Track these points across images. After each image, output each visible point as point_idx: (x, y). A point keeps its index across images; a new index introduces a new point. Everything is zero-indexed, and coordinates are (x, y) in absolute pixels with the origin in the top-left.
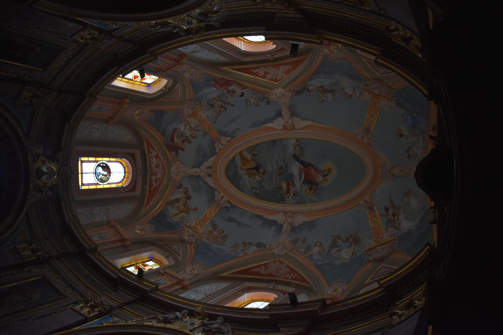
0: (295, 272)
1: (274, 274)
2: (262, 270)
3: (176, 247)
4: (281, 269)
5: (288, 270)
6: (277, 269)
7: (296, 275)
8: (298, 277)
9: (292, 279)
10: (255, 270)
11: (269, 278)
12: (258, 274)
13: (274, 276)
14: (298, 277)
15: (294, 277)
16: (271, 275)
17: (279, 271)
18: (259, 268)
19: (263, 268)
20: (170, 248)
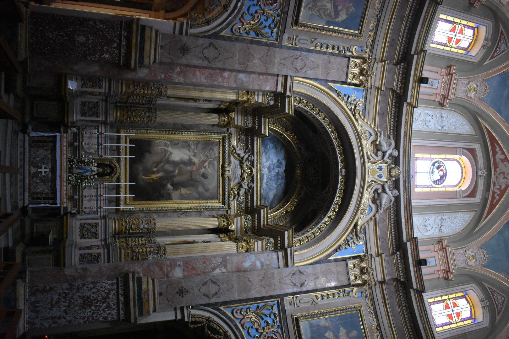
0: (501, 196)
1: (498, 170)
2: (499, 156)
3: (502, 47)
4: (505, 178)
5: (503, 187)
6: (504, 173)
7: (498, 198)
8: (495, 201)
9: (494, 193)
10: (498, 149)
11: (492, 166)
12: (495, 153)
13: (495, 170)
14: (495, 201)
15: (496, 195)
16: (496, 166)
17: (502, 175)
18: (500, 152)
19: (503, 157)
20: (500, 41)
